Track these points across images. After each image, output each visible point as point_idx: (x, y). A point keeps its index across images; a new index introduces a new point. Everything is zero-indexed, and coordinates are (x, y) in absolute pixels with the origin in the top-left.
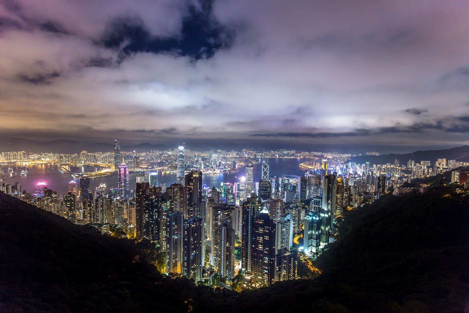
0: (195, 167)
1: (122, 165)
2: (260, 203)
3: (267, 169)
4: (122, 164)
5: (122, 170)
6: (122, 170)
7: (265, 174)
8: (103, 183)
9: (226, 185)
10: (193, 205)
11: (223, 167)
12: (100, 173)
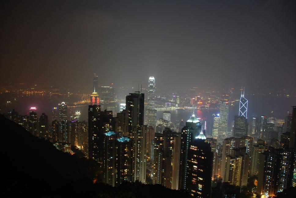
0: (171, 102)
1: (94, 94)
2: (200, 128)
3: (246, 105)
4: (93, 93)
5: (94, 98)
6: (94, 98)
7: (243, 109)
8: (79, 112)
11: (201, 103)
12: (80, 104)
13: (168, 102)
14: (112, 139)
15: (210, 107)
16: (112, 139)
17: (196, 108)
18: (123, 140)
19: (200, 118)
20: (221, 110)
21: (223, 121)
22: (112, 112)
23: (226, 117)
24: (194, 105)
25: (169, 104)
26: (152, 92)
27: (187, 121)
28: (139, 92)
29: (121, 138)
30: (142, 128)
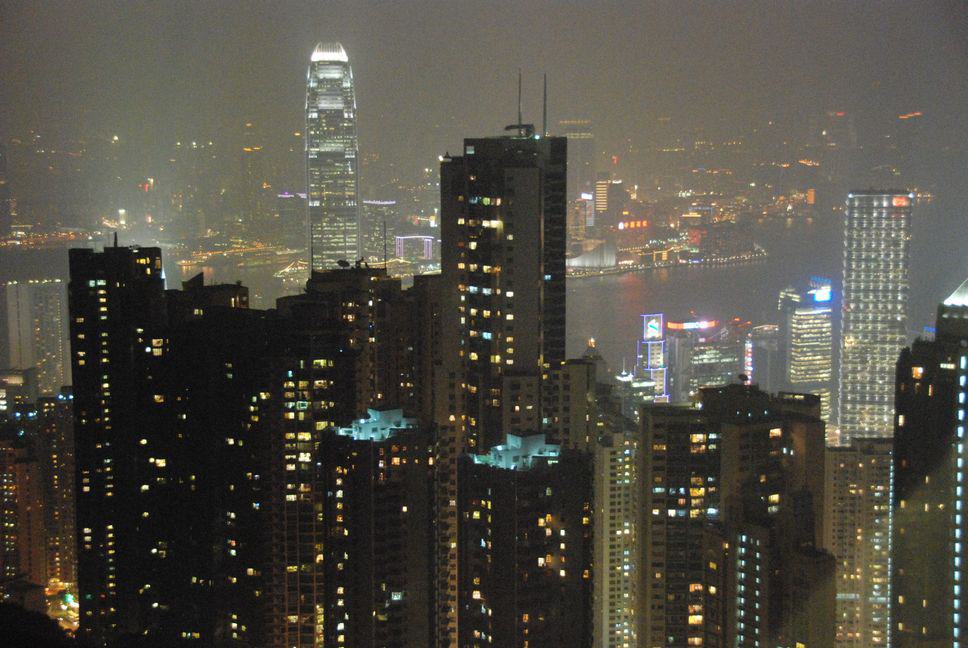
9: (682, 333)
10: (507, 380)
13: (408, 228)
14: (396, 461)
15: (706, 247)
16: (396, 461)
17: (613, 263)
18: (516, 459)
19: (710, 320)
20: (859, 260)
21: (874, 332)
22: (246, 294)
23: (895, 301)
24: (591, 245)
25: (419, 244)
26: (338, 156)
27: (948, 302)
28: (530, 129)
29: (500, 448)
30: (567, 377)
